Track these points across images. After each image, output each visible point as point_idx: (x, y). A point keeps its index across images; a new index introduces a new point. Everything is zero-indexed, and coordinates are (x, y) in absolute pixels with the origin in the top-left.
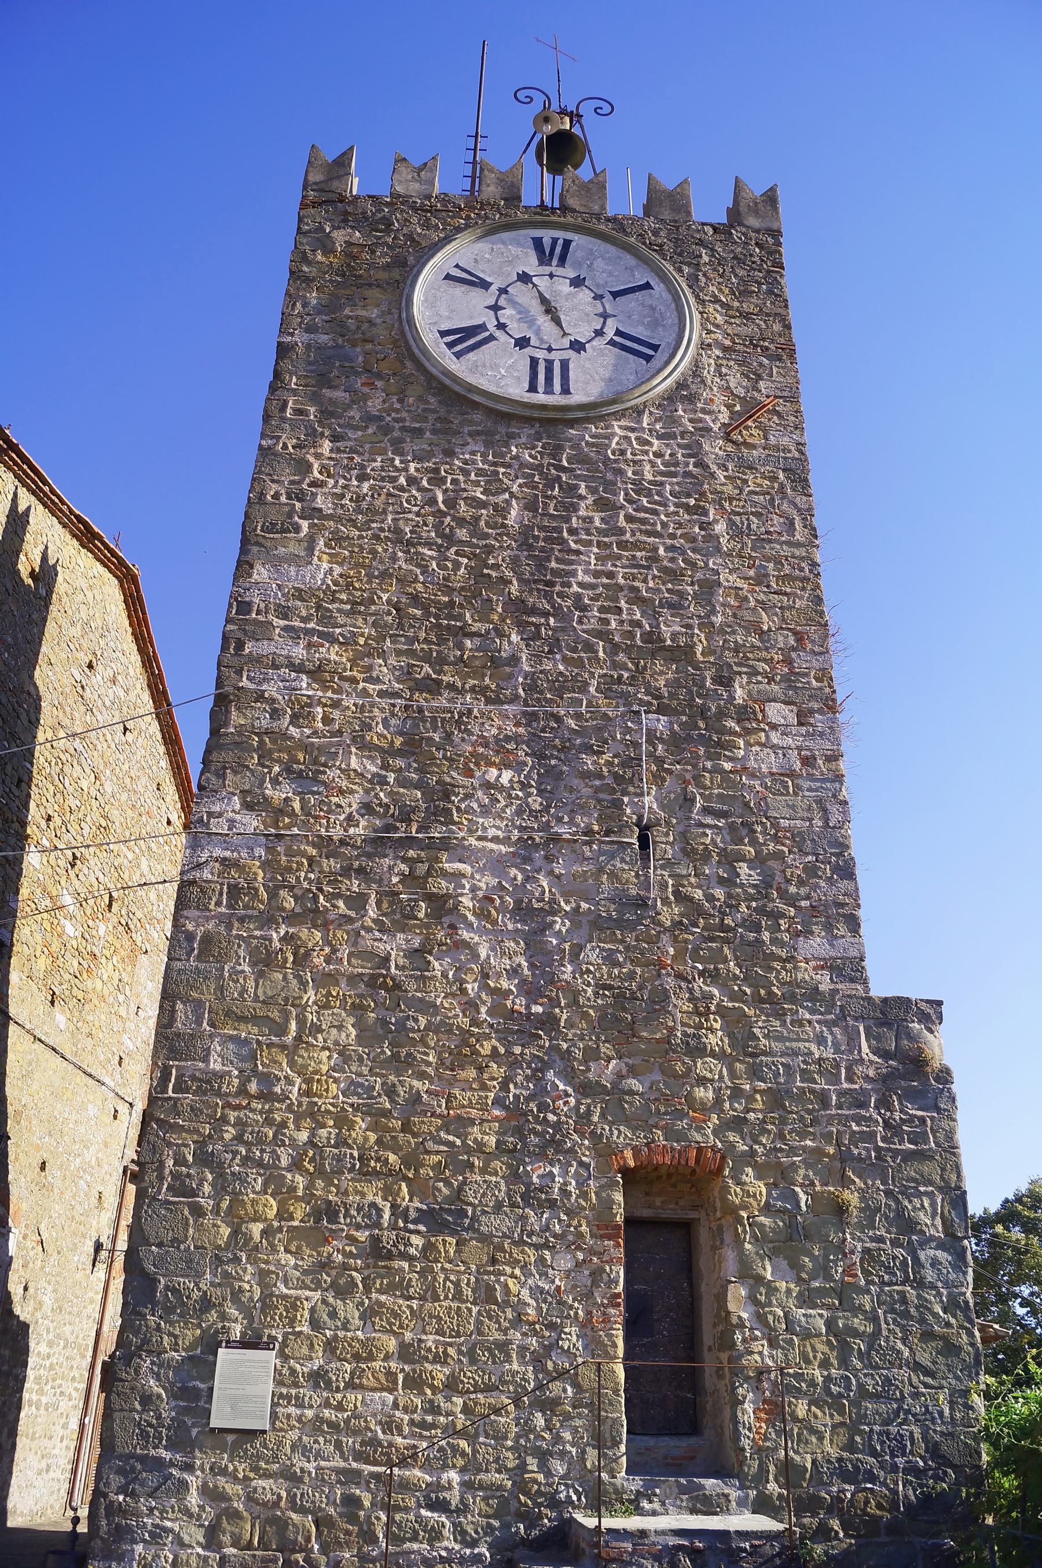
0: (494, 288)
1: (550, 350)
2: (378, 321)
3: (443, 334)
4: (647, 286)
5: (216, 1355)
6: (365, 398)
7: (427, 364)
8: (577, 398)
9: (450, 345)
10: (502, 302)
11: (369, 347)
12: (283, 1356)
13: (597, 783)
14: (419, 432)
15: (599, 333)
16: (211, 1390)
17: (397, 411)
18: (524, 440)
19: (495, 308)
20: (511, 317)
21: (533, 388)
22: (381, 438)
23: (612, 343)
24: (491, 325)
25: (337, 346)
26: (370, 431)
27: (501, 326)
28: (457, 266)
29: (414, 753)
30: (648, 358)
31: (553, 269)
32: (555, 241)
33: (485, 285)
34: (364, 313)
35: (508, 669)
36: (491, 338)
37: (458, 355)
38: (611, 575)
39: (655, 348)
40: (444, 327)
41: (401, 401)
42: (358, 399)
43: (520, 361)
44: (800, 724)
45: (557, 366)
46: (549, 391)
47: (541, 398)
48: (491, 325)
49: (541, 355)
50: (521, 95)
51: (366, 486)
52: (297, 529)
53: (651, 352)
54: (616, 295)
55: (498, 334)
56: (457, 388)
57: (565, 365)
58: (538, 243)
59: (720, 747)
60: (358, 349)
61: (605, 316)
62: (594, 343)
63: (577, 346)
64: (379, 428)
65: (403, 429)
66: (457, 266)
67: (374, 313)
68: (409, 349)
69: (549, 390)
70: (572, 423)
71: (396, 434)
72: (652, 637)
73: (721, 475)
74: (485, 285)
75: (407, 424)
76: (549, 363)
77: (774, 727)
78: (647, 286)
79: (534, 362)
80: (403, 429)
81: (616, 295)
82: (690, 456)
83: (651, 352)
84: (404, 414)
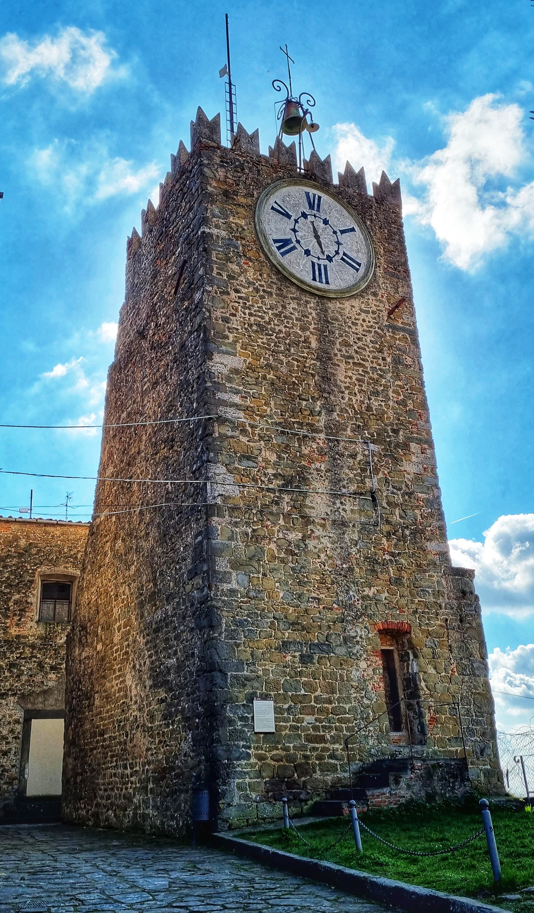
0: (293, 218)
1: (319, 258)
2: (246, 228)
3: (276, 241)
4: (353, 230)
5: (253, 704)
6: (246, 271)
7: (271, 258)
8: (332, 287)
9: (279, 248)
10: (296, 228)
11: (244, 242)
12: (275, 702)
13: (355, 472)
14: (270, 294)
15: (337, 253)
16: (253, 717)
17: (260, 281)
18: (312, 305)
19: (294, 230)
20: (301, 237)
21: (314, 279)
22: (256, 294)
23: (342, 259)
24: (294, 240)
25: (229, 239)
26: (251, 289)
27: (298, 242)
28: (276, 202)
29: (287, 453)
30: (357, 270)
31: (315, 212)
32: (314, 195)
33: (289, 217)
34: (239, 222)
35: (318, 417)
36: (294, 248)
37: (283, 254)
38: (351, 378)
39: (359, 265)
40: (275, 237)
41: (261, 275)
42: (244, 272)
43: (306, 262)
44: (422, 453)
45: (322, 267)
46: (321, 281)
47: (317, 284)
48: (294, 240)
49: (315, 260)
50: (276, 84)
51: (252, 319)
52: (227, 337)
53: (358, 267)
54: (343, 232)
55: (297, 245)
56: (285, 273)
57: (325, 267)
58: (307, 194)
59: (396, 460)
60: (239, 242)
61: (338, 243)
62: (336, 258)
63: (329, 258)
64: (254, 288)
65: (263, 290)
66: (276, 202)
67: (243, 222)
68: (262, 247)
69: (321, 281)
70: (330, 299)
71: (262, 293)
72: (369, 408)
73: (387, 334)
74: (289, 217)
75: (265, 288)
76: (319, 265)
77: (413, 453)
78: (353, 230)
79: (313, 264)
80: (263, 290)
81: (343, 232)
82: (377, 323)
83: (358, 267)
84: (263, 283)
